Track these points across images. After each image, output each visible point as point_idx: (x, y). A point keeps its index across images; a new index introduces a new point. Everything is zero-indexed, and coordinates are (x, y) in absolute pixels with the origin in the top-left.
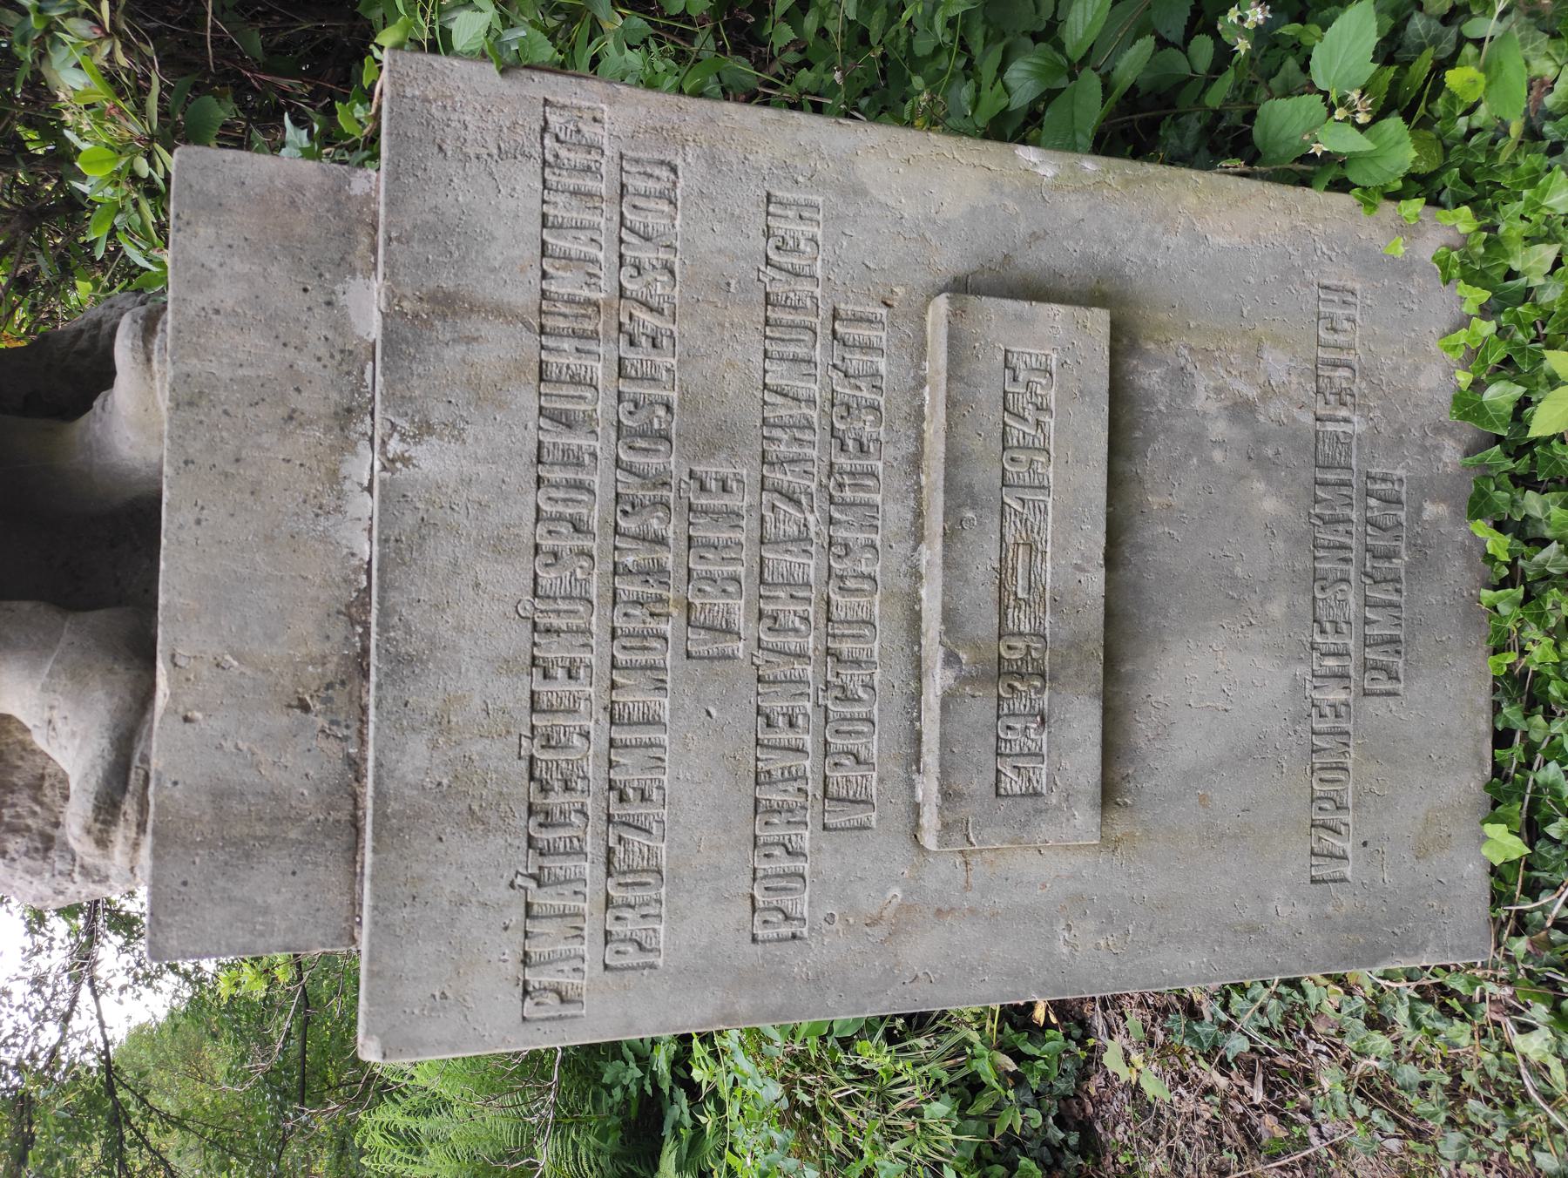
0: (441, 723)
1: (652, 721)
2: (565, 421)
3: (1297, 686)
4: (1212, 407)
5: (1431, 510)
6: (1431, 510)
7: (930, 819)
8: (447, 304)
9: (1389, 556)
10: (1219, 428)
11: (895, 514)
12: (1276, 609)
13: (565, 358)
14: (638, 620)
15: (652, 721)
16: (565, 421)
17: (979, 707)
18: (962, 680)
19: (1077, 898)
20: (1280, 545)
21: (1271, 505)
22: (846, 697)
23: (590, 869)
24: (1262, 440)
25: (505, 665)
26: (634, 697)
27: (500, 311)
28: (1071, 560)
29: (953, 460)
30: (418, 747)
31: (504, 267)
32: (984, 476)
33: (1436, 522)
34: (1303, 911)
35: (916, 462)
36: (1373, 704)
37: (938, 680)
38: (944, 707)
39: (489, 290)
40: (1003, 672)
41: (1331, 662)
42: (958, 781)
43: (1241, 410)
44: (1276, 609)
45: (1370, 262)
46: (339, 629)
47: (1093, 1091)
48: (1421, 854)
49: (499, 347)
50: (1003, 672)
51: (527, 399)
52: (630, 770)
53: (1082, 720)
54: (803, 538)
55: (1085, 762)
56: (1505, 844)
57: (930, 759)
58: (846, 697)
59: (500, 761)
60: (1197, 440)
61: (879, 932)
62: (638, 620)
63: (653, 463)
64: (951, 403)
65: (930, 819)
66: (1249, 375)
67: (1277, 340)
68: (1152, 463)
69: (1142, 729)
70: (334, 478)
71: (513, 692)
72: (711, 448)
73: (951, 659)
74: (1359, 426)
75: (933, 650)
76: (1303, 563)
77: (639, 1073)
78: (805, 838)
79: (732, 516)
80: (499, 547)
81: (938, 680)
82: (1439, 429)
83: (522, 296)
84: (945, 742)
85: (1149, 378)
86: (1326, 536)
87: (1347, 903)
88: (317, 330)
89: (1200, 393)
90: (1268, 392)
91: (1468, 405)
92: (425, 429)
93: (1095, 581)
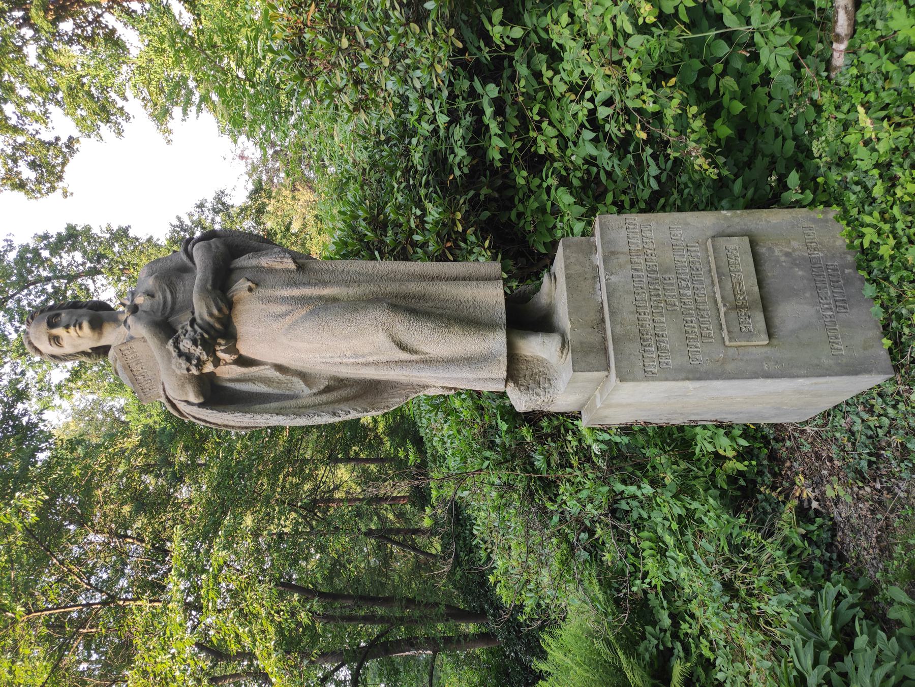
0: (622, 323)
1: (662, 322)
2: (637, 270)
3: (818, 311)
4: (780, 254)
5: (847, 271)
6: (847, 271)
7: (727, 338)
8: (613, 253)
9: (837, 282)
10: (783, 258)
11: (708, 282)
12: (808, 295)
13: (635, 260)
14: (656, 304)
15: (662, 322)
16: (637, 270)
17: (733, 314)
18: (728, 309)
19: (767, 357)
20: (805, 281)
21: (800, 273)
22: (702, 317)
23: (654, 349)
24: (795, 260)
25: (632, 313)
26: (657, 318)
27: (622, 253)
28: (749, 284)
29: (717, 268)
30: (618, 327)
31: (622, 246)
32: (725, 270)
33: (849, 273)
34: (831, 362)
35: (710, 271)
36: (840, 315)
37: (723, 310)
38: (725, 314)
39: (620, 250)
40: (737, 307)
41: (826, 306)
42: (731, 329)
43: (787, 254)
44: (808, 295)
45: (815, 221)
46: (598, 314)
47: (839, 539)
48: (865, 349)
49: (623, 259)
50: (737, 307)
51: (629, 267)
52: (659, 332)
53: (759, 317)
54: (688, 287)
55: (762, 325)
56: (887, 343)
57: (724, 326)
58: (702, 317)
59: (634, 329)
60: (778, 261)
61: (719, 363)
62: (656, 304)
63: (655, 276)
64: (715, 258)
65: (727, 338)
66: (789, 247)
67: (794, 239)
68: (767, 267)
69: (777, 321)
70: (594, 288)
71: (634, 317)
72: (666, 272)
73: (725, 305)
74: (821, 254)
75: (720, 304)
76: (813, 284)
77: (656, 642)
78: (699, 344)
79: (672, 284)
80: (628, 292)
81: (723, 310)
82: (844, 253)
83: (626, 250)
84: (726, 321)
85: (762, 250)
86: (818, 279)
87: (845, 360)
88: (588, 264)
89: (775, 252)
90: (794, 250)
91: (850, 246)
92: (612, 274)
93: (756, 288)
